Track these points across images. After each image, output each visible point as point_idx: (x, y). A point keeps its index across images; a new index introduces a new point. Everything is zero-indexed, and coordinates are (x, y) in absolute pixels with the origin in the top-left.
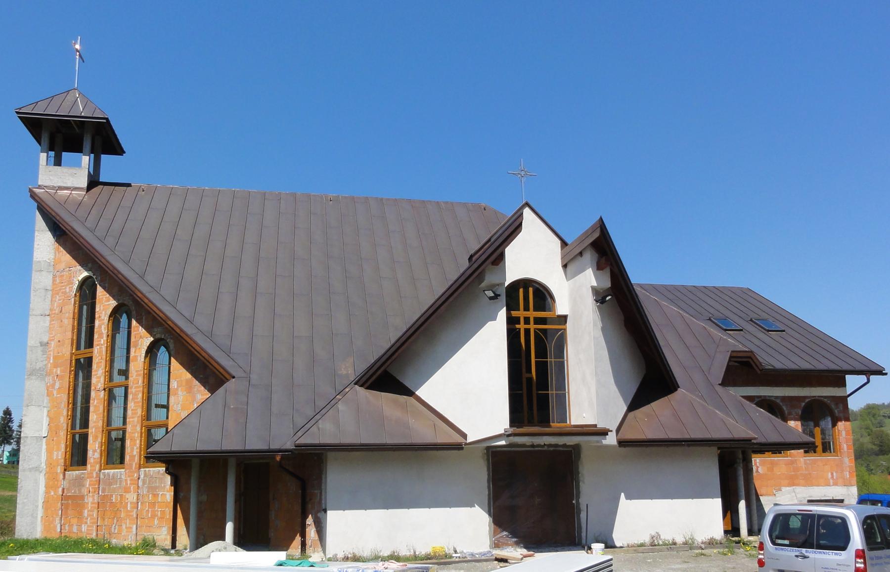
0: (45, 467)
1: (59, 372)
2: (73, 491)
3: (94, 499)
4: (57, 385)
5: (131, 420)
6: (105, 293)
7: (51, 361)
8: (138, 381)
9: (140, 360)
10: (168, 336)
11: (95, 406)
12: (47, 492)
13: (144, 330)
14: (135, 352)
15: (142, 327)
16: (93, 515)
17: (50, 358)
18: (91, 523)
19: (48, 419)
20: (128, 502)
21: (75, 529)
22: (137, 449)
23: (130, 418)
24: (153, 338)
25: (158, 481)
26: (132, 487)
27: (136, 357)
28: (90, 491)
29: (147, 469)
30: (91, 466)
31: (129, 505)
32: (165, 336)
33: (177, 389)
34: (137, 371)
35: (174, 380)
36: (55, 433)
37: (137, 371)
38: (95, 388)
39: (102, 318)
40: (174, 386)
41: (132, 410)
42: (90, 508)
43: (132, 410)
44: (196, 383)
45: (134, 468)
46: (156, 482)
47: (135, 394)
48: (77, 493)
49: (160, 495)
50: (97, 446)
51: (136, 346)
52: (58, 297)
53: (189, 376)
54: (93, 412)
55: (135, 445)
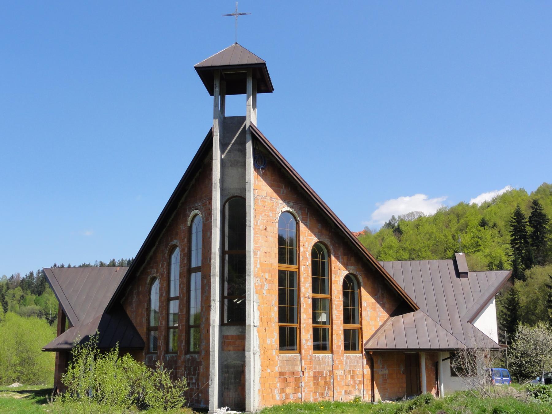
0: (259, 350)
1: (267, 277)
2: (287, 369)
3: (309, 374)
4: (266, 286)
5: (336, 322)
6: (307, 229)
7: (258, 266)
8: (339, 297)
9: (340, 284)
10: (359, 273)
11: (305, 309)
12: (263, 370)
13: (341, 265)
14: (335, 277)
15: (339, 262)
16: (309, 386)
17: (257, 264)
18: (308, 391)
19: (258, 312)
20: (337, 376)
21: (291, 397)
22: (341, 341)
23: (335, 320)
24: (348, 271)
25: (355, 362)
26: (340, 366)
27: (336, 281)
28: (305, 369)
29: (348, 355)
30: (305, 351)
31: (338, 378)
32: (356, 273)
33: (366, 307)
34: (338, 291)
35: (364, 301)
36: (267, 323)
37: (338, 291)
38: (304, 296)
39: (306, 246)
40: (364, 305)
41: (336, 315)
42: (306, 381)
43: (336, 315)
44: (378, 305)
45: (340, 354)
46: (354, 363)
47: (338, 306)
48: (291, 370)
49: (358, 371)
50: (309, 337)
51: (336, 274)
52: (261, 217)
53: (373, 301)
54: (303, 312)
55: (340, 338)
